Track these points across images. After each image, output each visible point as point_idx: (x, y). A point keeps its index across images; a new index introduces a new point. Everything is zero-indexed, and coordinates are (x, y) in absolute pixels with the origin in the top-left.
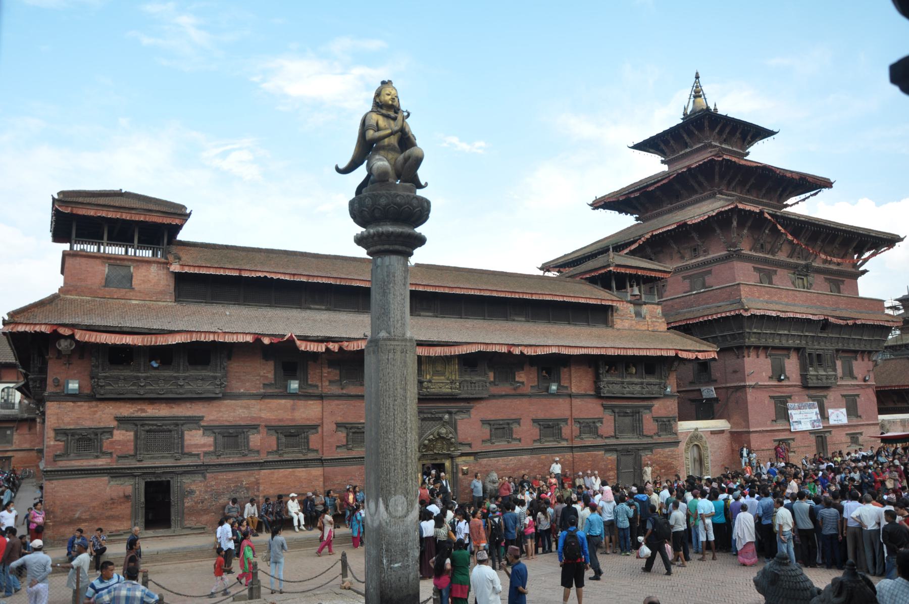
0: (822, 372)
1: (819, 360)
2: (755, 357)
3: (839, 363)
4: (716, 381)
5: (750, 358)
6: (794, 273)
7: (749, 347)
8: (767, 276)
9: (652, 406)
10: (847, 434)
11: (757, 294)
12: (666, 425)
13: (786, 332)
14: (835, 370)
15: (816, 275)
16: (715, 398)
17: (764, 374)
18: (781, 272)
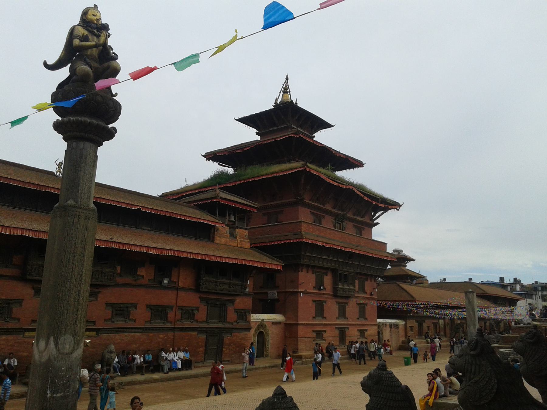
0: (346, 287)
3: (357, 282)
5: (303, 273)
6: (335, 220)
7: (303, 265)
8: (318, 220)
9: (235, 300)
10: (358, 330)
11: (311, 230)
12: (243, 315)
13: (327, 257)
14: (354, 286)
16: (277, 299)
17: (310, 285)
18: (327, 217)
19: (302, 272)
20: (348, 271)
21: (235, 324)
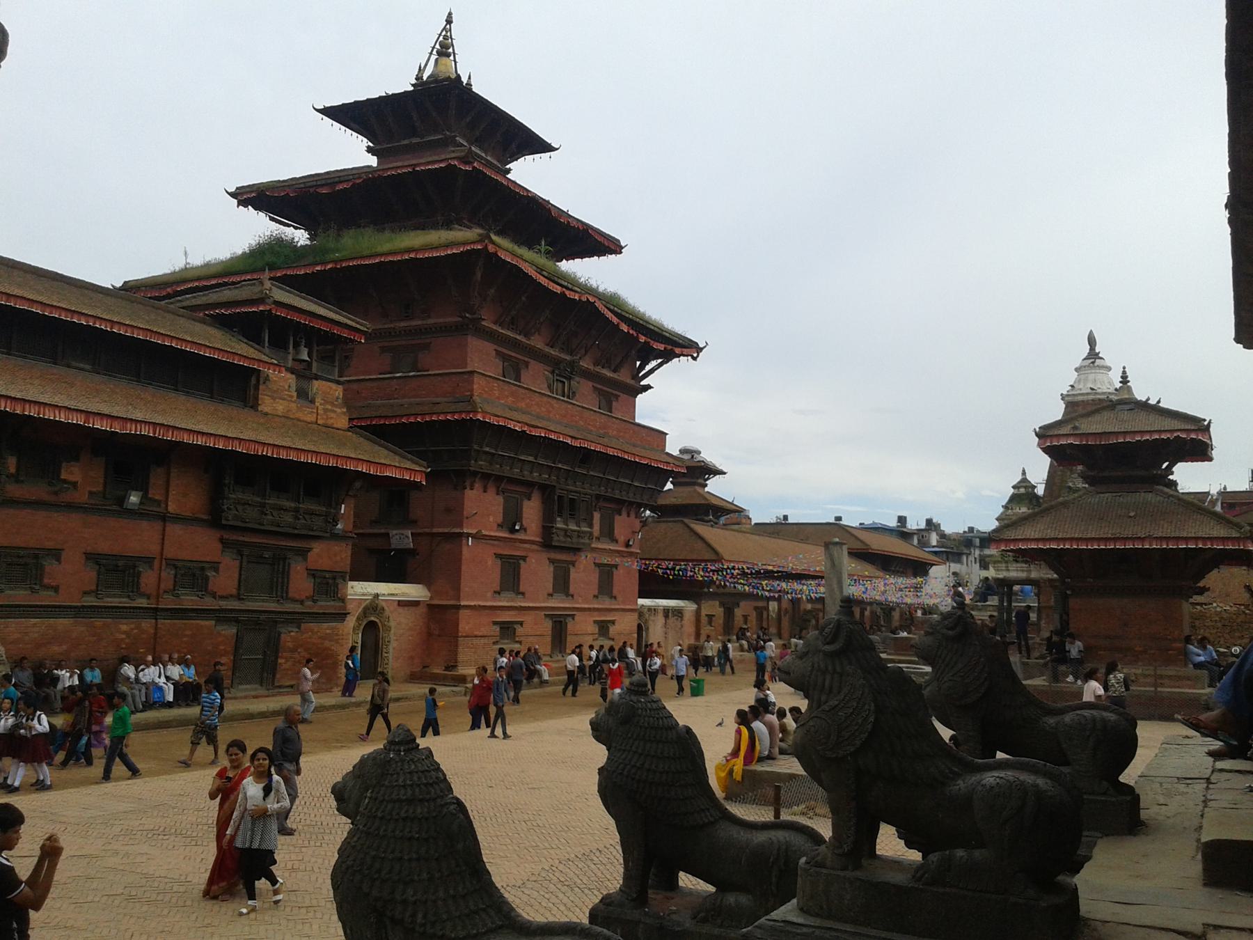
0: (573, 527)
1: (570, 508)
2: (482, 490)
3: (597, 516)
4: (415, 522)
6: (553, 372)
7: (475, 474)
8: (513, 370)
9: (310, 550)
10: (595, 622)
11: (497, 393)
12: (329, 584)
13: (531, 459)
14: (591, 526)
15: (583, 381)
16: (410, 549)
17: (491, 519)
19: (472, 489)
20: (579, 493)
21: (310, 603)
